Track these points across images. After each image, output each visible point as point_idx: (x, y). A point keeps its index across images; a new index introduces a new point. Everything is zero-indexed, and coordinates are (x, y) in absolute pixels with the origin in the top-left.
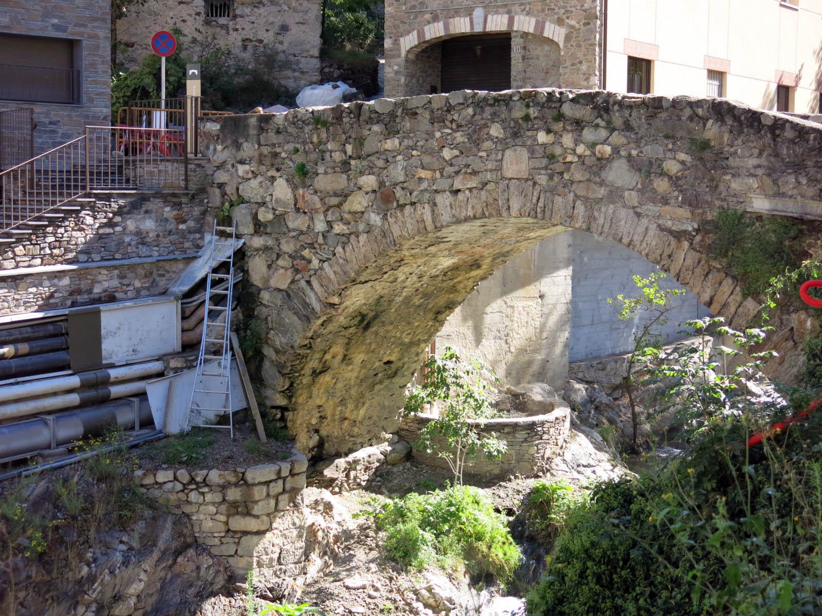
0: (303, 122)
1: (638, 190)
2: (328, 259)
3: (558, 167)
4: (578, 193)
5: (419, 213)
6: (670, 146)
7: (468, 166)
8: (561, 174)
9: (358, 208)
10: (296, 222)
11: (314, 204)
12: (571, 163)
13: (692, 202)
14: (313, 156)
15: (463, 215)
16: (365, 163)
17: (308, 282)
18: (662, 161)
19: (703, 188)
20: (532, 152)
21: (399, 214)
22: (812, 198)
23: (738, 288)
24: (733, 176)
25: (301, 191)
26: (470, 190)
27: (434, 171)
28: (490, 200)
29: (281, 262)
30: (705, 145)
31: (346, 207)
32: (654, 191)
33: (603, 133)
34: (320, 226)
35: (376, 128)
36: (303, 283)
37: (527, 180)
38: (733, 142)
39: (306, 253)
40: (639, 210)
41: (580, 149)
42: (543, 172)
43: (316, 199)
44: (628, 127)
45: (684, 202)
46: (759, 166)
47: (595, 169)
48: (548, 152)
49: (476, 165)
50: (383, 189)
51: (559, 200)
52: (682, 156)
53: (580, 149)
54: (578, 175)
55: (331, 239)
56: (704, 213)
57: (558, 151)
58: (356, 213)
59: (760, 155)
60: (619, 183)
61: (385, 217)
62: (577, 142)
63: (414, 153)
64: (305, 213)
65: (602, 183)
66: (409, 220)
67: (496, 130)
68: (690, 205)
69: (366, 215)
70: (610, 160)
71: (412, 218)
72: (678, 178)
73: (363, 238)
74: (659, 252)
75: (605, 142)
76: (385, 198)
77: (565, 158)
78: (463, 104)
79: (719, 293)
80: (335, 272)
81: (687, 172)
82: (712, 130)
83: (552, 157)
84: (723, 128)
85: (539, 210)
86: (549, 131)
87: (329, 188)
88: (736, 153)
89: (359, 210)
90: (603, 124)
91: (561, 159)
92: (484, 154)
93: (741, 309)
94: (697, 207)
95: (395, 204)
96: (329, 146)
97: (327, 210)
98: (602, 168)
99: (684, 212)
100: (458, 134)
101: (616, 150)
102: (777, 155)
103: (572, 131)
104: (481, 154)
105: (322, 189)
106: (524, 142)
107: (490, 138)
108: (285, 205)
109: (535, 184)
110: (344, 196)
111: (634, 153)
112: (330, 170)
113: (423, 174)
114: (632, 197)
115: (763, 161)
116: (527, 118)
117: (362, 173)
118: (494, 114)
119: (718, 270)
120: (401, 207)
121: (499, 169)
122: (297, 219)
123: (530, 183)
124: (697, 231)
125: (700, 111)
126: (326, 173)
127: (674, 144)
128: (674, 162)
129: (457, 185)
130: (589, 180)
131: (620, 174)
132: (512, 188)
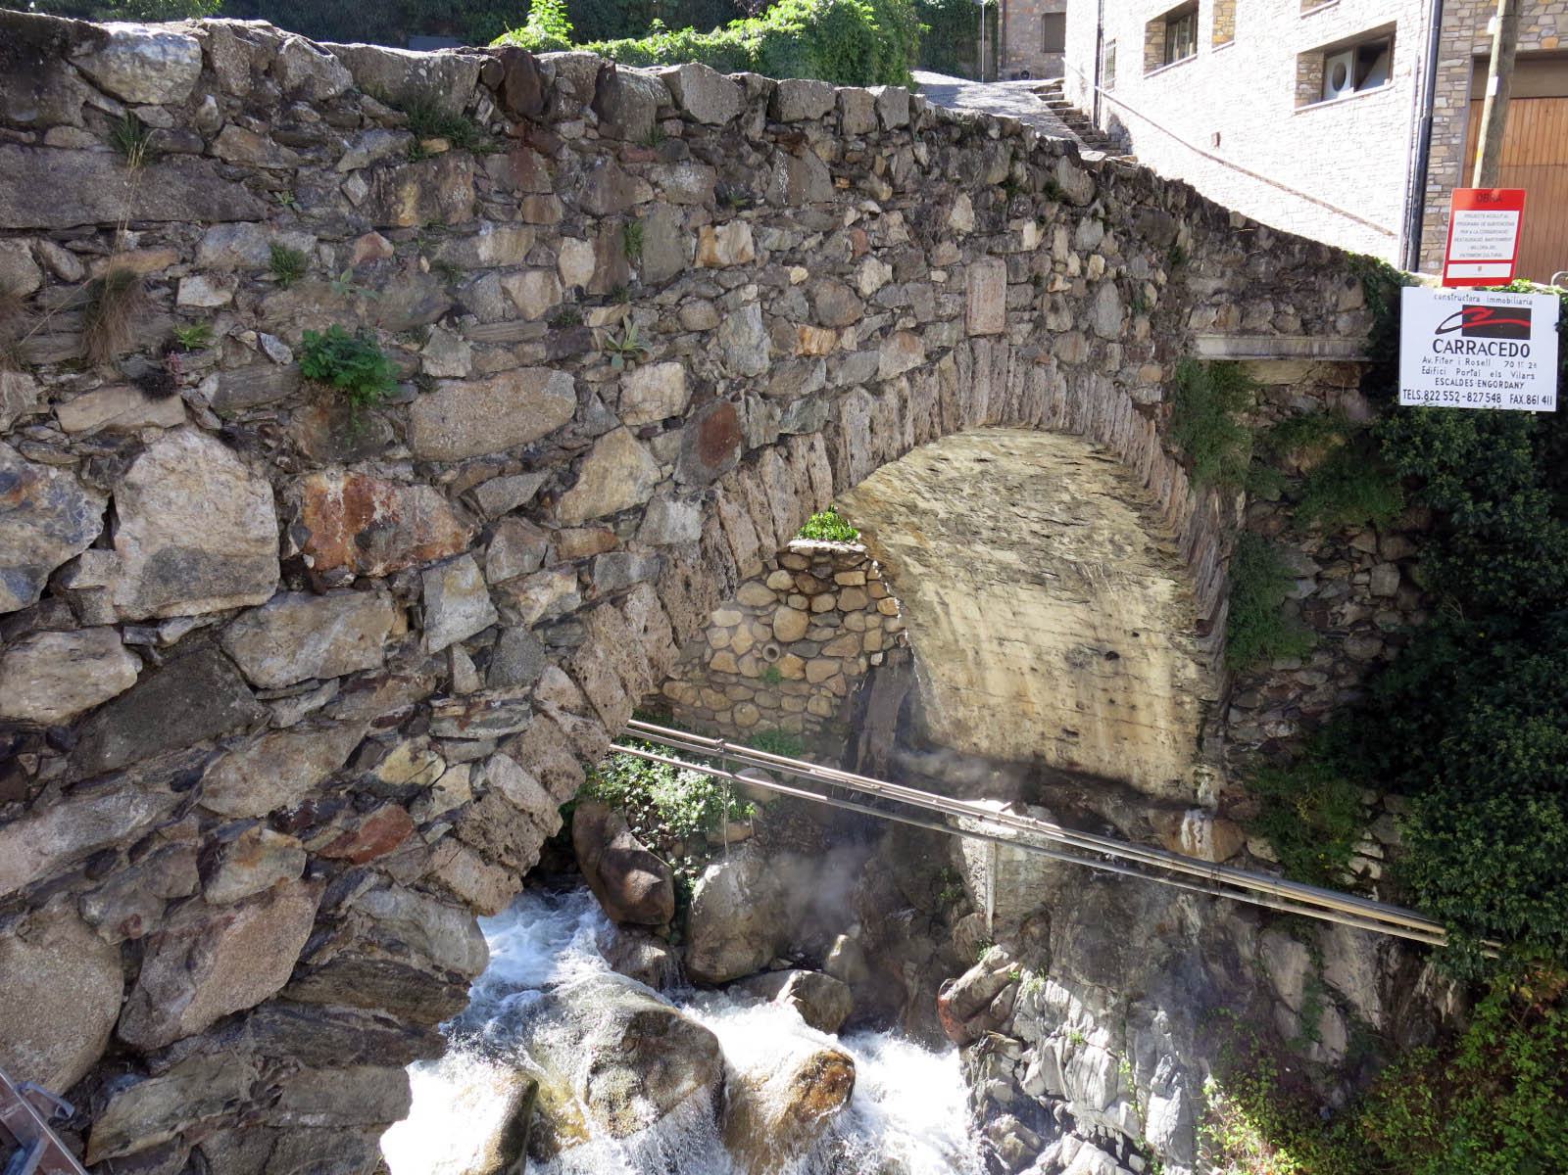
0: (323, 106)
5: (801, 465)
7: (907, 310)
9: (623, 493)
10: (287, 649)
11: (425, 525)
14: (404, 296)
15: (897, 445)
16: (645, 316)
17: (430, 886)
20: (1013, 268)
21: (749, 484)
22: (1295, 333)
25: (332, 484)
26: (911, 375)
27: (839, 330)
29: (236, 881)
31: (576, 503)
35: (690, 179)
38: (1196, 250)
39: (395, 766)
40: (1121, 378)
42: (1026, 316)
43: (428, 498)
49: (925, 309)
50: (708, 409)
55: (517, 652)
58: (613, 518)
59: (1223, 274)
61: (708, 504)
62: (1072, 247)
63: (798, 273)
64: (362, 582)
66: (776, 495)
69: (653, 516)
71: (783, 489)
73: (642, 602)
76: (713, 439)
77: (1053, 282)
78: (905, 128)
80: (545, 782)
85: (1015, 401)
87: (494, 441)
89: (630, 501)
92: (938, 276)
95: (738, 452)
96: (486, 248)
97: (482, 540)
100: (896, 218)
105: (461, 446)
106: (1006, 247)
107: (952, 234)
108: (229, 569)
110: (560, 458)
112: (501, 358)
113: (817, 340)
117: (635, 359)
118: (965, 168)
120: (752, 458)
121: (963, 316)
122: (319, 626)
126: (478, 375)
131: (1108, 311)
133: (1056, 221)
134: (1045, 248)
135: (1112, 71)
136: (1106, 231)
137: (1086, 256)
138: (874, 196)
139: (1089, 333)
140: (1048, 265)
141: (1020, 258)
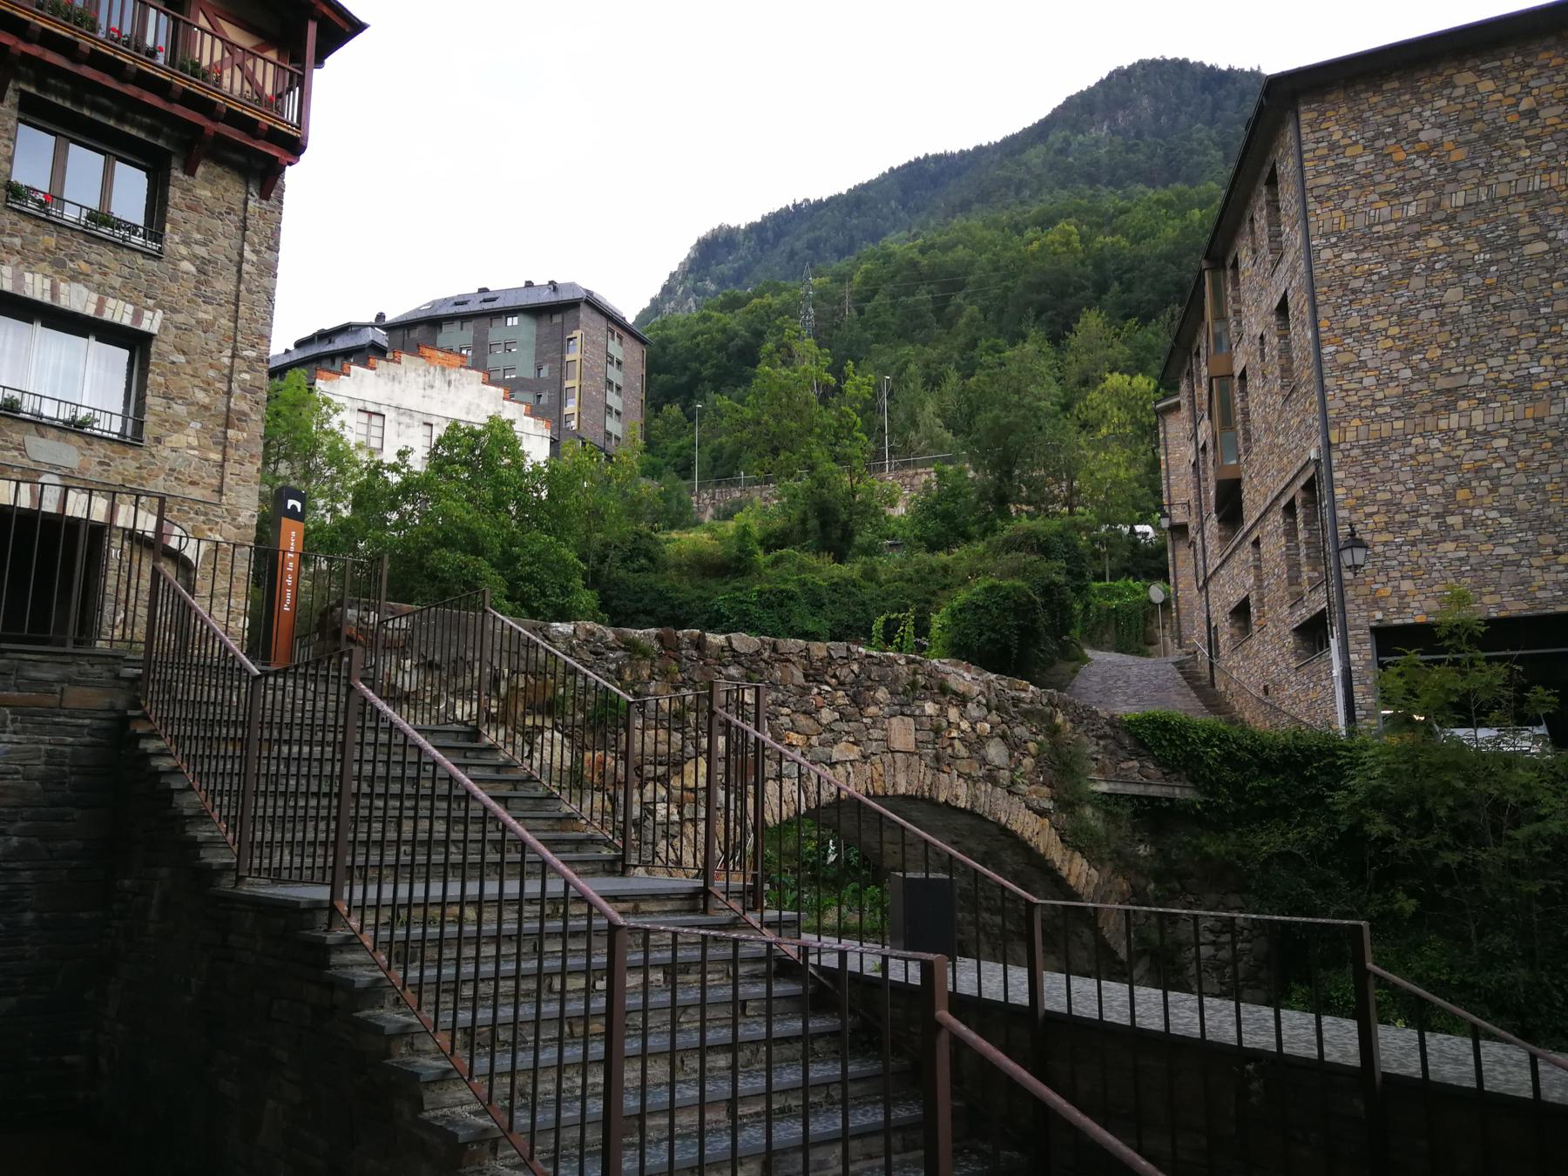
37: (912, 754)
54: (962, 751)
63: (785, 711)
67: (882, 694)
83: (937, 731)
92: (868, 721)
99: (1045, 790)
113: (795, 738)
116: (914, 684)
129: (836, 756)
131: (996, 752)
132: (899, 764)
134: (943, 712)
135: (1217, 647)
136: (990, 711)
138: (827, 684)
139: (984, 761)
140: (945, 724)
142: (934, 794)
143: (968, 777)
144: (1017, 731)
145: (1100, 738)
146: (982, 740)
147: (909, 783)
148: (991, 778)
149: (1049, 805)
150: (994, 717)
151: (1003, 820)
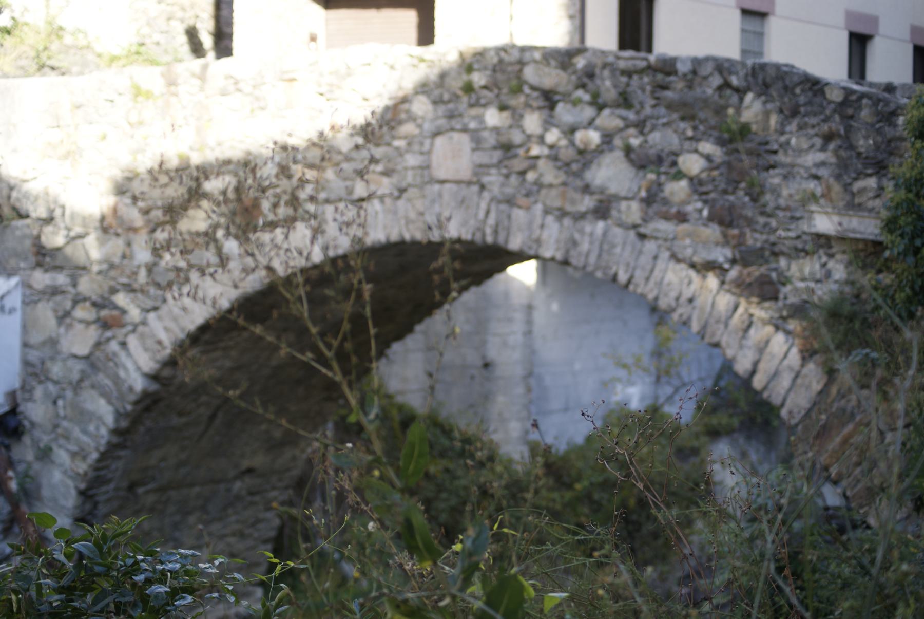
1: (642, 200)
2: (155, 309)
3: (518, 164)
4: (549, 203)
6: (690, 133)
8: (523, 173)
12: (537, 158)
13: (725, 219)
17: (123, 344)
18: (676, 154)
19: (741, 197)
23: (794, 351)
24: (785, 177)
28: (412, 215)
29: (81, 313)
30: (745, 131)
32: (666, 202)
33: (589, 112)
34: (143, 255)
36: (114, 346)
37: (469, 183)
38: (783, 125)
39: (121, 299)
40: (642, 230)
41: (552, 136)
44: (625, 101)
45: (711, 219)
46: (823, 164)
47: (575, 167)
48: (503, 139)
51: (519, 215)
52: (707, 147)
53: (552, 136)
54: (549, 174)
56: (742, 235)
57: (517, 138)
60: (613, 189)
62: (548, 124)
64: (117, 235)
65: (587, 189)
68: (721, 223)
70: (599, 151)
72: (701, 183)
74: (673, 294)
75: (590, 124)
77: (528, 150)
79: (766, 357)
81: (715, 173)
82: (752, 109)
83: (507, 148)
84: (769, 106)
86: (503, 108)
88: (788, 143)
90: (587, 97)
91: (521, 152)
93: (799, 381)
94: (730, 225)
97: (153, 231)
98: (586, 165)
99: (713, 232)
101: (608, 138)
102: (851, 147)
103: (539, 108)
104: (397, 143)
109: (483, 187)
111: (635, 142)
114: (632, 211)
115: (827, 156)
116: (469, 88)
119: (765, 323)
123: (475, 188)
124: (733, 262)
125: (734, 81)
127: (695, 128)
128: (695, 157)
130: (564, 184)
131: (611, 173)
132: (446, 197)
133: (527, 106)
137: (571, 131)
139: (587, 189)
141: (485, 134)
142: (501, 240)
143: (562, 214)
144: (655, 137)
145: (828, 138)
146: (586, 157)
147: (464, 223)
148: (602, 211)
149: (721, 255)
150: (609, 119)
151: (623, 277)
